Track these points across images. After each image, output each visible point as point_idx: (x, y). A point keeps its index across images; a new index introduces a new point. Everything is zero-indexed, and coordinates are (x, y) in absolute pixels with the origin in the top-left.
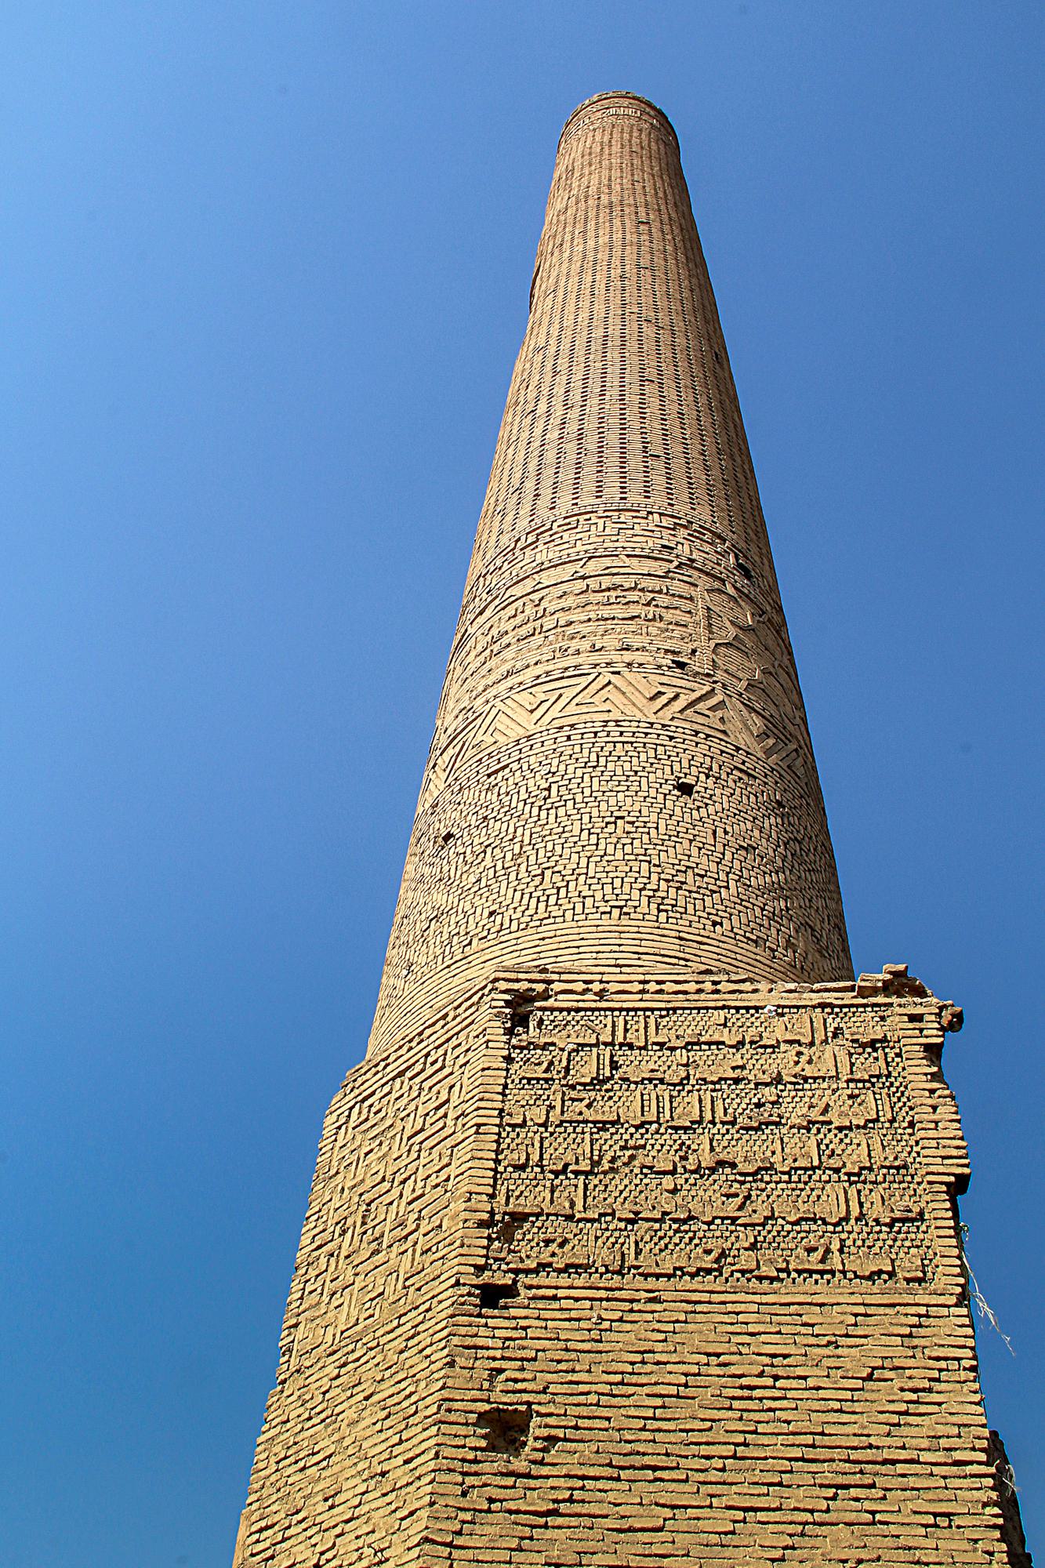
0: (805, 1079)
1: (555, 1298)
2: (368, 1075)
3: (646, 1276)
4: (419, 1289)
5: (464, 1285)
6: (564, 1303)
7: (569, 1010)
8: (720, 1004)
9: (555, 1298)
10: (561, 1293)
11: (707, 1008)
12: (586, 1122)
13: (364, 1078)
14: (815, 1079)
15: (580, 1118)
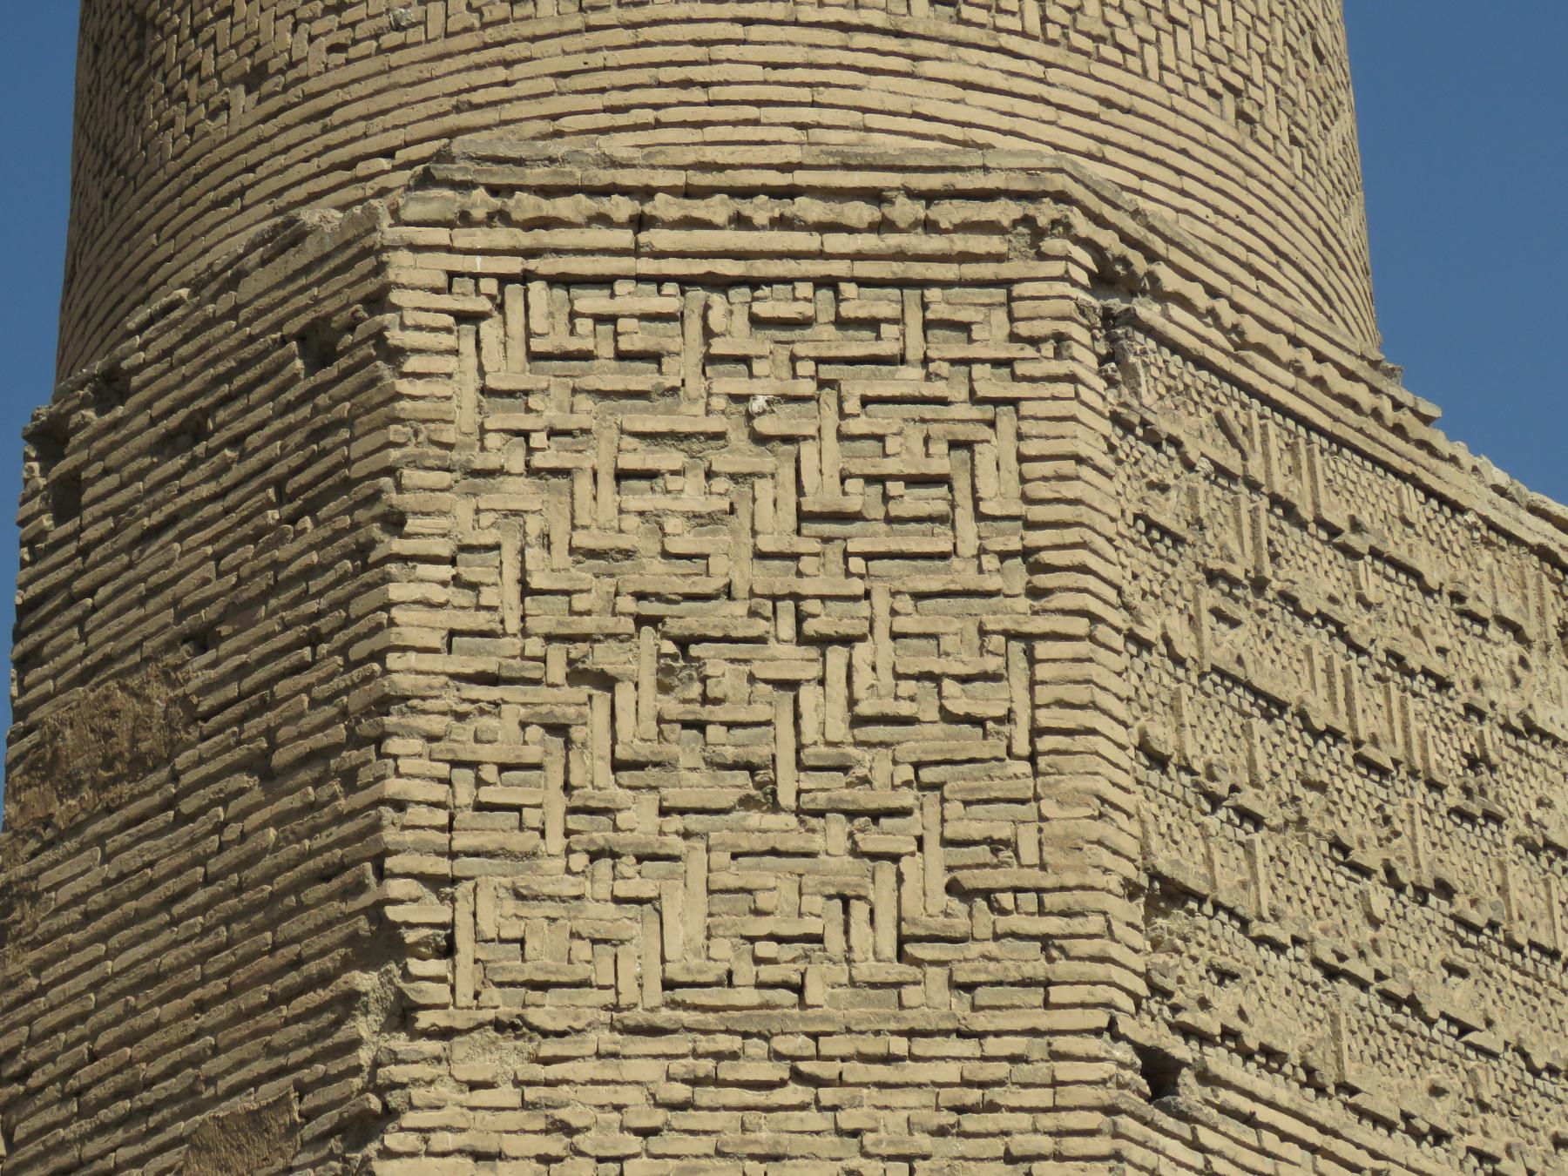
0: (1531, 728)
1: (1249, 1120)
2: (562, 207)
3: (1362, 1113)
4: (969, 987)
5: (1117, 1037)
6: (1270, 1141)
7: (1176, 348)
8: (1408, 468)
9: (1249, 1120)
10: (1264, 1114)
11: (1388, 468)
12: (1248, 687)
13: (551, 207)
14: (1544, 735)
15: (1237, 671)
